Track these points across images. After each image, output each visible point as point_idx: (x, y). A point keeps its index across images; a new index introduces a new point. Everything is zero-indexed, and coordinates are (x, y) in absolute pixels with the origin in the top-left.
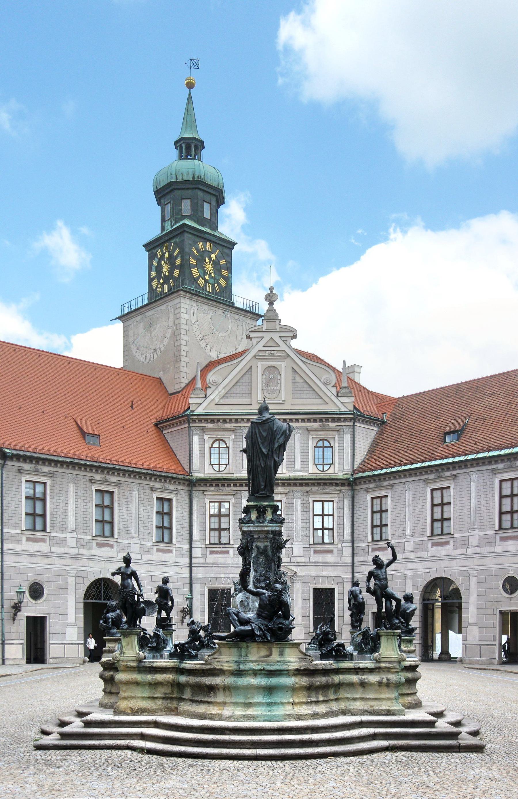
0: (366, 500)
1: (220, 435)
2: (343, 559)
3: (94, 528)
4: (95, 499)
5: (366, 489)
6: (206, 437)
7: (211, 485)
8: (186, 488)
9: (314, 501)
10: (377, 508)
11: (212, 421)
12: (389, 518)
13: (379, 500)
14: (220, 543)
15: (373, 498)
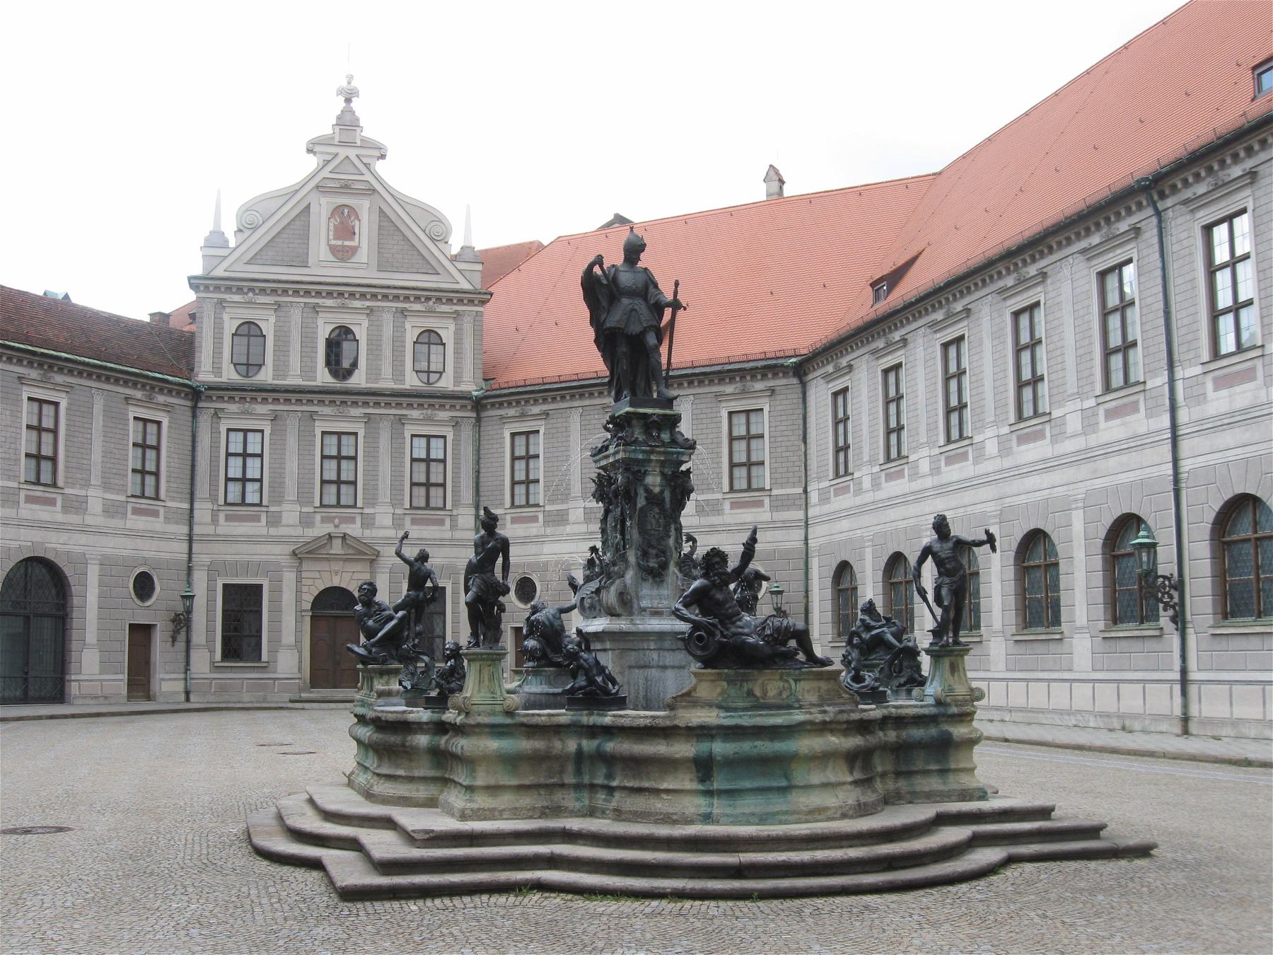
0: (502, 437)
1: (249, 314)
2: (458, 535)
3: (24, 468)
4: (27, 414)
5: (502, 417)
6: (226, 317)
7: (232, 398)
8: (189, 403)
9: (413, 436)
10: (520, 451)
11: (240, 290)
12: (539, 469)
13: (523, 438)
14: (243, 503)
15: (513, 435)
